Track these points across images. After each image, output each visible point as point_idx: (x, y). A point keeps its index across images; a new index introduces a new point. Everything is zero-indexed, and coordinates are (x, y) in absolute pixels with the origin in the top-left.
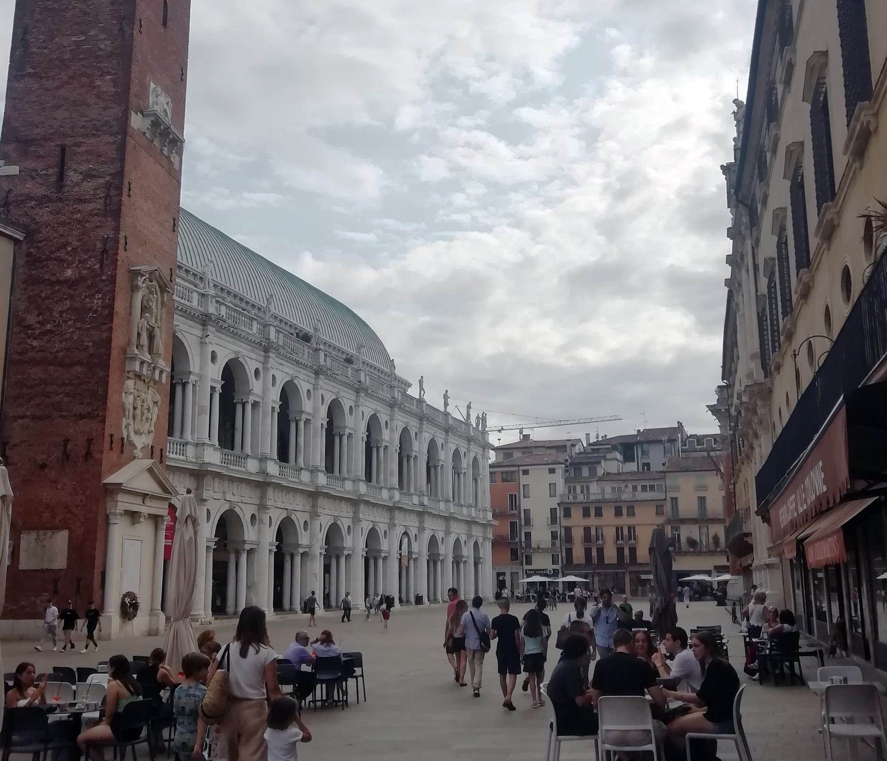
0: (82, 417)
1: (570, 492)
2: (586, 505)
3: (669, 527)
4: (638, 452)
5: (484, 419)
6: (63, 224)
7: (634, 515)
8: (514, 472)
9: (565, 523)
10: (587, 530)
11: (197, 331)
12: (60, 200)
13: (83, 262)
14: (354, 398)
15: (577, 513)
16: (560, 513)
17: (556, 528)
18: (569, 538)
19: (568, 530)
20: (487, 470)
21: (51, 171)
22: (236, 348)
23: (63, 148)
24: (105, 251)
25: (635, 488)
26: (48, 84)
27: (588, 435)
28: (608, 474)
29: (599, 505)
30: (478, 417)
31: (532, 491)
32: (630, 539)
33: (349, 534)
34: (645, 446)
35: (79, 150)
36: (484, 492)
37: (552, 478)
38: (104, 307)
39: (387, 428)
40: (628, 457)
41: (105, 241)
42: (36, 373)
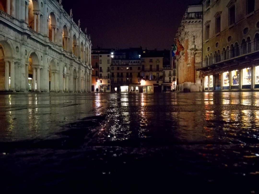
2: (118, 66)
9: (112, 71)
10: (118, 73)
17: (109, 73)
19: (113, 73)
33: (42, 60)
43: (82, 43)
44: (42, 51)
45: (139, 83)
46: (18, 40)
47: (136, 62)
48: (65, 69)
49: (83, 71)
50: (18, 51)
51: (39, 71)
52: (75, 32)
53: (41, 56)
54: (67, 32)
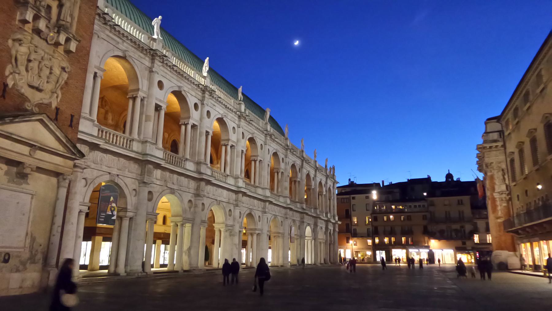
5: (334, 168)
8: (348, 198)
9: (375, 224)
11: (147, 62)
14: (264, 139)
20: (335, 196)
22: (179, 84)
27: (383, 182)
30: (331, 168)
36: (334, 206)
39: (283, 162)
43: (320, 183)
44: (260, 209)
45: (426, 245)
46: (231, 201)
47: (420, 206)
48: (293, 228)
49: (321, 228)
50: (230, 215)
51: (255, 237)
52: (309, 169)
53: (259, 216)
54: (296, 172)
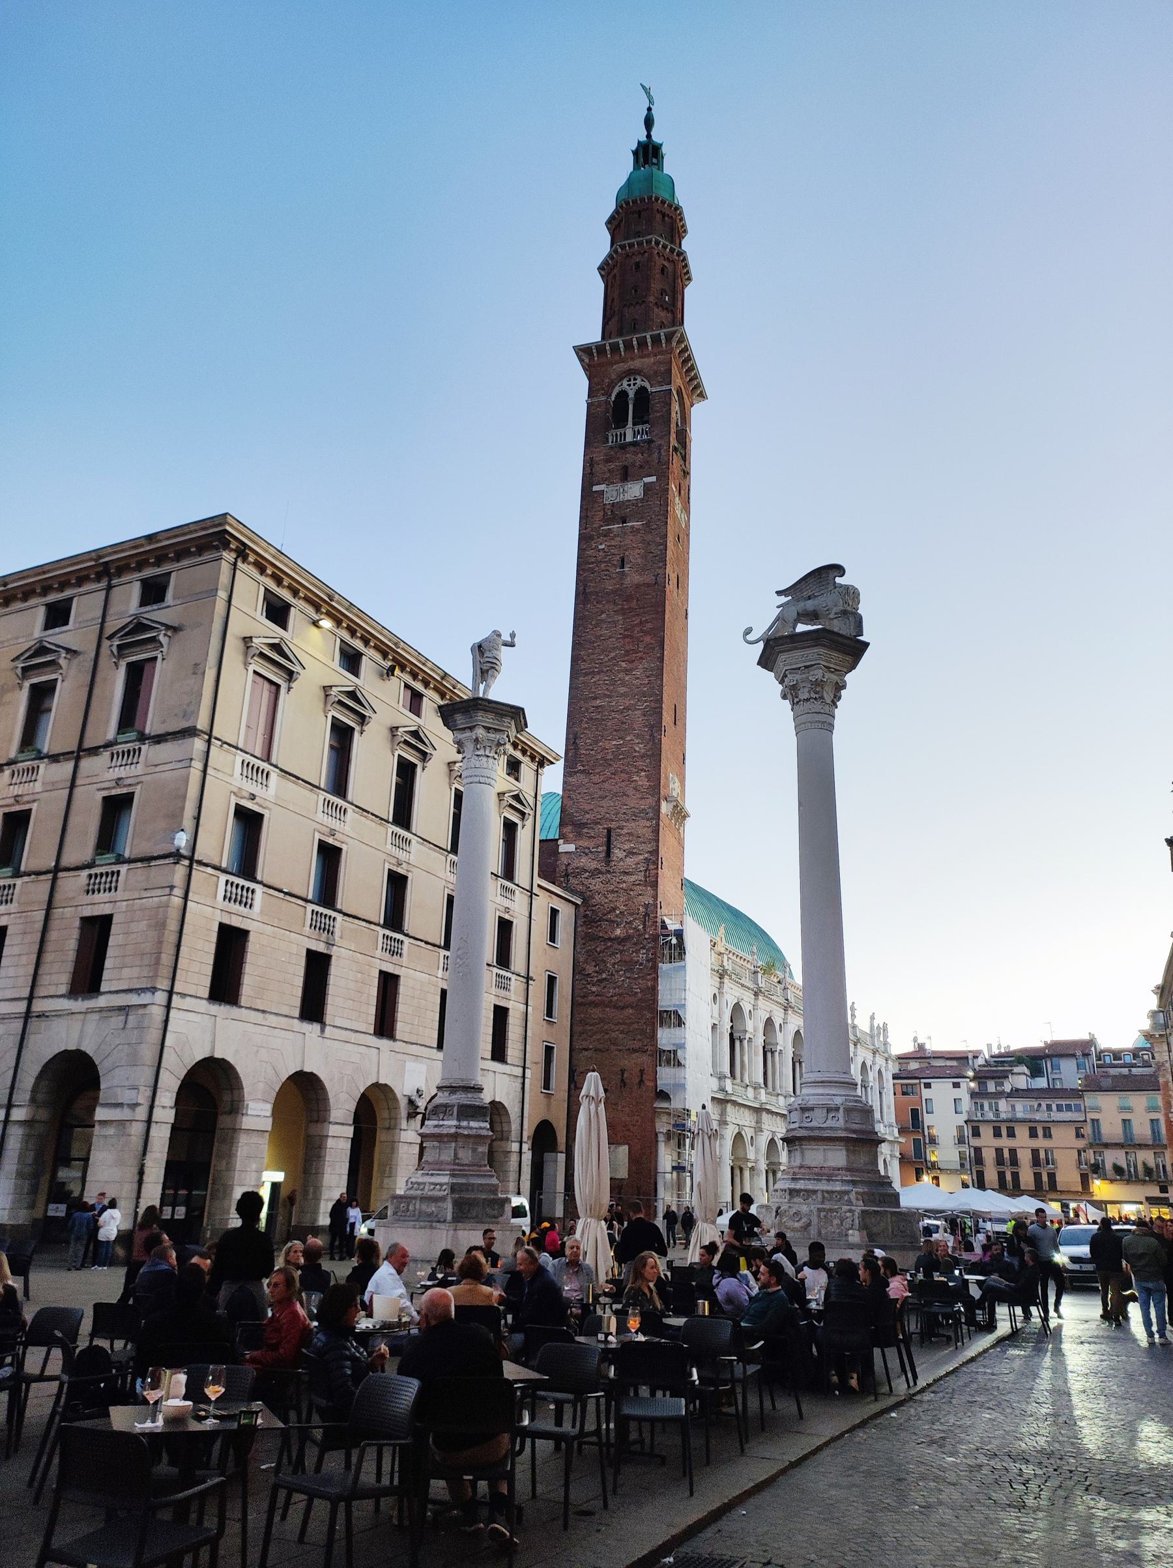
0: (635, 1051)
1: (976, 1109)
3: (1091, 1151)
4: (1047, 1065)
6: (612, 892)
7: (1050, 1136)
9: (975, 1142)
10: (999, 1151)
12: (608, 872)
13: (631, 922)
15: (987, 1132)
16: (968, 1131)
17: (965, 1148)
18: (979, 1160)
19: (978, 1150)
20: (891, 1081)
21: (600, 849)
23: (609, 831)
24: (647, 914)
25: (1049, 1107)
26: (596, 779)
28: (1017, 1090)
29: (1012, 1124)
31: (936, 1106)
32: (1048, 1163)
34: (1054, 1059)
35: (623, 832)
36: (889, 1107)
37: (957, 1093)
38: (648, 961)
40: (1036, 1072)
41: (646, 906)
42: (596, 1013)
